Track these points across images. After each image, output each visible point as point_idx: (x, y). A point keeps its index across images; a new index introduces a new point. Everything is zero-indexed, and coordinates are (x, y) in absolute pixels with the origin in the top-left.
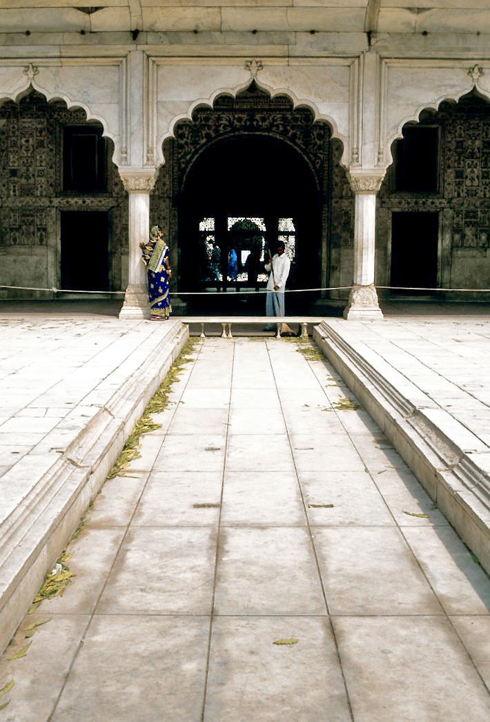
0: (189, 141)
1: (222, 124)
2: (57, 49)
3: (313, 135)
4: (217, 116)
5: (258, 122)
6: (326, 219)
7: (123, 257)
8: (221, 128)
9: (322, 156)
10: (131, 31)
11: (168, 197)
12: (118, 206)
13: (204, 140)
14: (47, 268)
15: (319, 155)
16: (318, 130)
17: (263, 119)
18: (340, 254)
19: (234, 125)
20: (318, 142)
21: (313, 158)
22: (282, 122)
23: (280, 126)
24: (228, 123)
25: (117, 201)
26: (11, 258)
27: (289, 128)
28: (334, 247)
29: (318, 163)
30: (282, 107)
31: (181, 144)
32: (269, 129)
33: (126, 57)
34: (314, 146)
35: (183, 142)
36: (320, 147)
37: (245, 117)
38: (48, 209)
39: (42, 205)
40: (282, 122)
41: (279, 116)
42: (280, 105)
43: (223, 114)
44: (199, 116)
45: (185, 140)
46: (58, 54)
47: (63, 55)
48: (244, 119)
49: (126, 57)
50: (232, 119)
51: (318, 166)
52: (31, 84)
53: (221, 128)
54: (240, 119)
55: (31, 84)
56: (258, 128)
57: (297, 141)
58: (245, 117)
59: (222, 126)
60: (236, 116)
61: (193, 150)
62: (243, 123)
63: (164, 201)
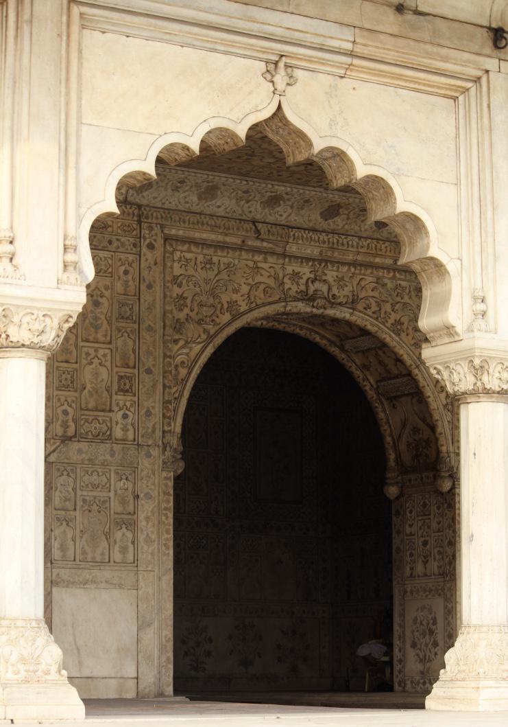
0: (193, 314)
2: (348, 34)
4: (251, 264)
5: (330, 289)
7: (55, 590)
10: (490, 29)
13: (226, 317)
19: (286, 287)
24: (271, 282)
27: (388, 307)
30: (377, 260)
31: (178, 320)
33: (477, 80)
35: (181, 316)
41: (371, 279)
42: (376, 255)
43: (265, 260)
44: (215, 259)
45: (186, 311)
46: (349, 46)
47: (359, 49)
48: (305, 278)
49: (477, 80)
50: (281, 275)
52: (279, 107)
53: (260, 293)
54: (296, 276)
55: (279, 107)
56: (332, 302)
58: (306, 271)
59: (262, 286)
60: (289, 269)
61: (204, 337)
62: (303, 288)
63: (149, 455)
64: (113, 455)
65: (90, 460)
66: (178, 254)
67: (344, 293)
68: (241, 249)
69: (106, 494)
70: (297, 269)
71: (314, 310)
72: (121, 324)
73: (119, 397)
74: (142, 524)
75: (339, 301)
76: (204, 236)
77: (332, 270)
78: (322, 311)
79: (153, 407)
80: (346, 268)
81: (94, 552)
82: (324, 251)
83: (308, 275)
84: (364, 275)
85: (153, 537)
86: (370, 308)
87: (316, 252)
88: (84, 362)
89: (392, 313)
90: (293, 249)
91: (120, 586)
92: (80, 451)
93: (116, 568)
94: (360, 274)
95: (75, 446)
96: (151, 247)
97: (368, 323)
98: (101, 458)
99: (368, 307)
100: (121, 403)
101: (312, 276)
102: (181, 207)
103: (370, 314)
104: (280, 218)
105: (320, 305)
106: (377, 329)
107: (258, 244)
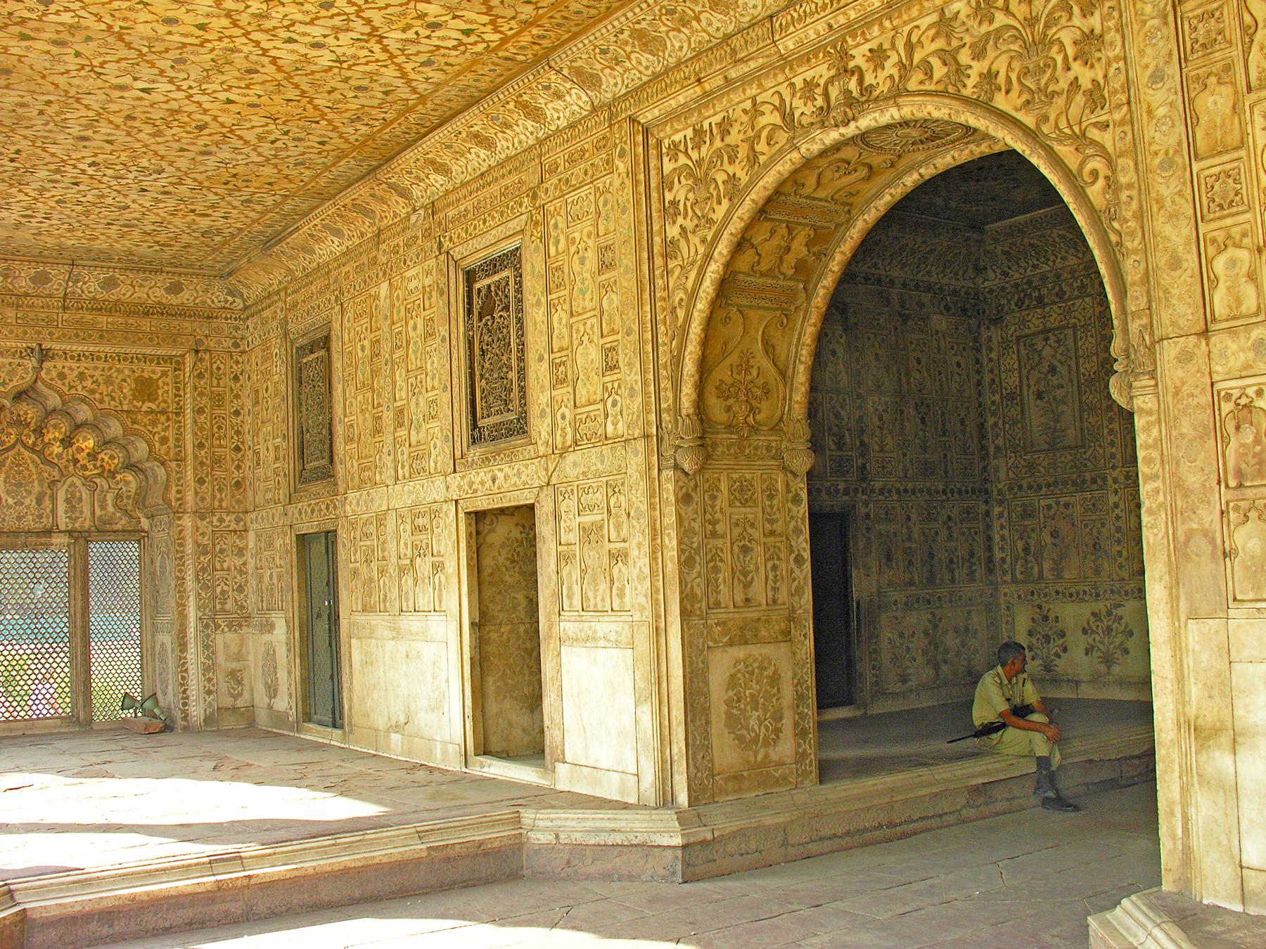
1: (764, 127)
3: (1062, 48)
6: (1155, 454)
8: (761, 147)
9: (1106, 138)
11: (646, 436)
12: (548, 484)
14: (447, 680)
15: (1094, 134)
16: (1077, 21)
17: (877, 56)
18: (1227, 653)
20: (1085, 76)
21: (1072, 161)
22: (940, 43)
23: (935, 62)
25: (546, 470)
26: (402, 646)
28: (1194, 615)
29: (1095, 174)
32: (898, 93)
34: (1069, 102)
36: (1096, 97)
37: (821, 71)
38: (445, 506)
39: (437, 499)
40: (940, 43)
51: (1095, 192)
57: (1000, 102)
64: (602, 462)
65: (584, 473)
66: (666, 142)
67: (887, 72)
68: (728, 93)
69: (599, 518)
70: (808, 75)
71: (842, 130)
72: (603, 277)
73: (607, 379)
74: (634, 553)
75: (875, 94)
76: (681, 99)
77: (858, 45)
78: (852, 125)
79: (636, 381)
80: (876, 30)
81: (595, 597)
82: (832, 22)
83: (827, 75)
84: (912, 20)
85: (647, 570)
86: (931, 77)
87: (821, 27)
88: (575, 343)
89: (973, 63)
90: (788, 44)
91: (617, 645)
92: (575, 464)
93: (613, 619)
94: (906, 23)
95: (570, 458)
96: (622, 154)
97: (930, 108)
98: (593, 468)
99: (929, 72)
100: (610, 385)
101: (833, 72)
102: (645, 79)
103: (933, 87)
104: (755, 13)
105: (840, 118)
106: (947, 111)
107: (744, 68)
